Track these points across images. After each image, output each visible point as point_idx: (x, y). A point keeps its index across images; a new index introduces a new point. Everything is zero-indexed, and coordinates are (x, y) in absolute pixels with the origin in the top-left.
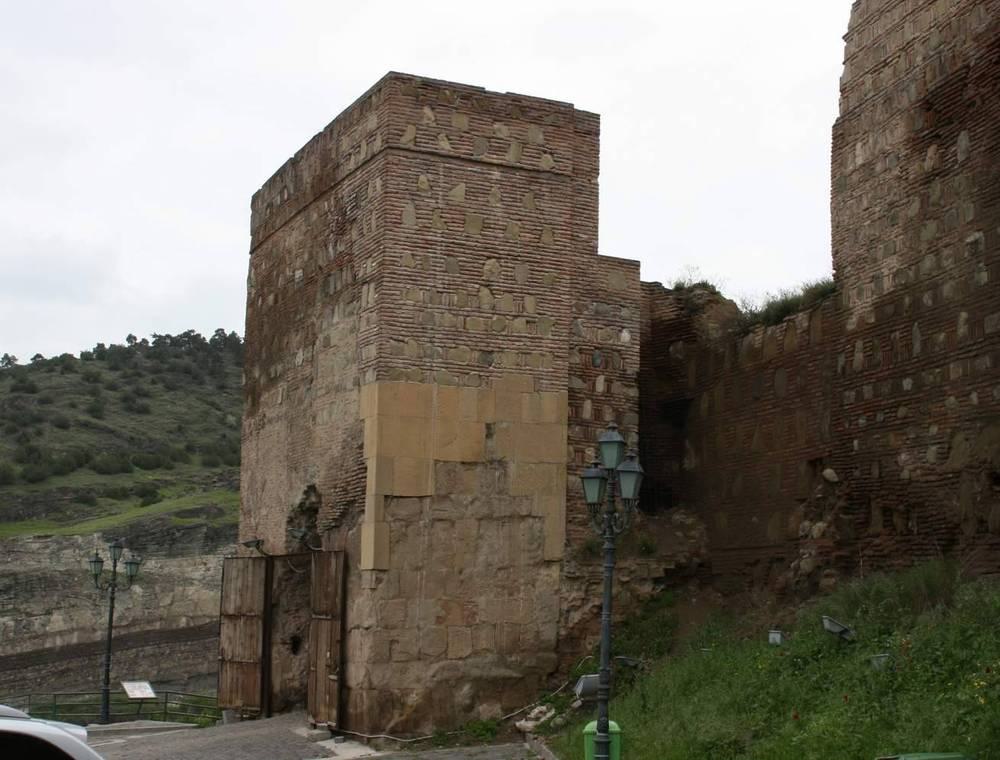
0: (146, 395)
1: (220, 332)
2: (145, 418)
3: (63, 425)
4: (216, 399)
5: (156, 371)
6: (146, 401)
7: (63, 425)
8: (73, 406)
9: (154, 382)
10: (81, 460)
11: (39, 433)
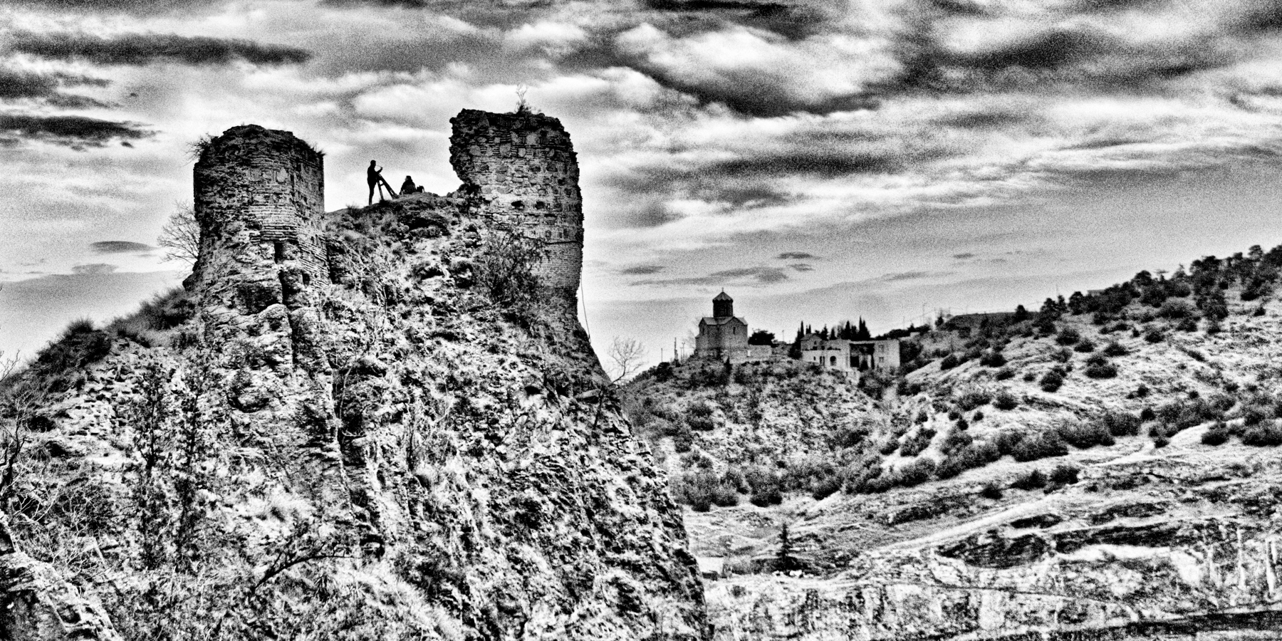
3: (1006, 404)
4: (1202, 350)
5: (1147, 318)
6: (1118, 360)
8: (1029, 378)
9: (1136, 334)
10: (1008, 446)
11: (979, 417)
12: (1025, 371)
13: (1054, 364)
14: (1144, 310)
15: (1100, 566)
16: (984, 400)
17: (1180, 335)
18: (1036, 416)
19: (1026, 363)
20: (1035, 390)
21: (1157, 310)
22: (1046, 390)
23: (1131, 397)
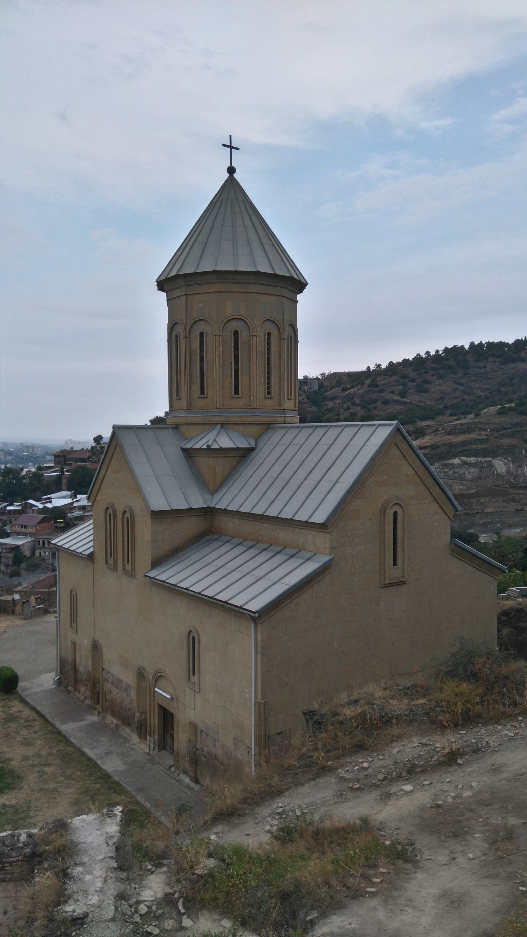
0: (429, 382)
1: (472, 344)
2: (426, 394)
3: (386, 402)
4: (462, 381)
6: (428, 386)
7: (386, 402)
8: (392, 392)
9: (433, 375)
11: (375, 408)
12: (390, 390)
13: (401, 387)
14: (433, 366)
15: (460, 466)
16: (376, 401)
17: (451, 376)
18: (398, 407)
19: (390, 386)
20: (396, 398)
21: (439, 366)
22: (402, 397)
23: (437, 400)
